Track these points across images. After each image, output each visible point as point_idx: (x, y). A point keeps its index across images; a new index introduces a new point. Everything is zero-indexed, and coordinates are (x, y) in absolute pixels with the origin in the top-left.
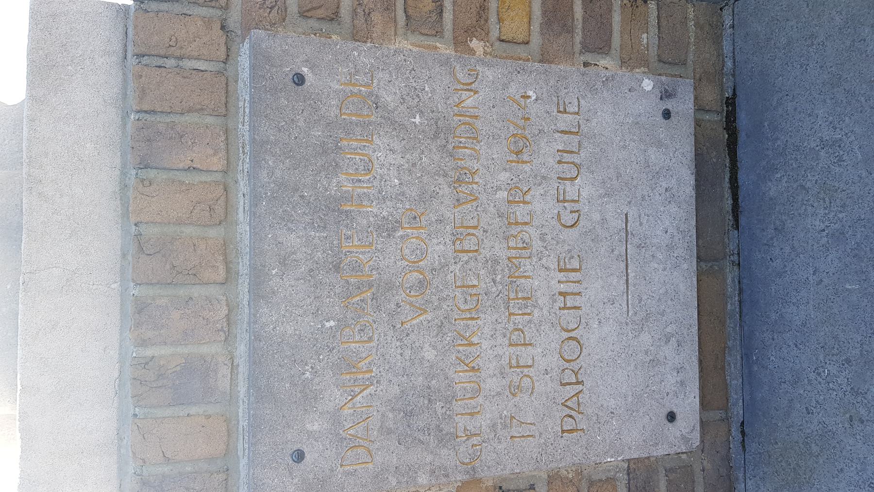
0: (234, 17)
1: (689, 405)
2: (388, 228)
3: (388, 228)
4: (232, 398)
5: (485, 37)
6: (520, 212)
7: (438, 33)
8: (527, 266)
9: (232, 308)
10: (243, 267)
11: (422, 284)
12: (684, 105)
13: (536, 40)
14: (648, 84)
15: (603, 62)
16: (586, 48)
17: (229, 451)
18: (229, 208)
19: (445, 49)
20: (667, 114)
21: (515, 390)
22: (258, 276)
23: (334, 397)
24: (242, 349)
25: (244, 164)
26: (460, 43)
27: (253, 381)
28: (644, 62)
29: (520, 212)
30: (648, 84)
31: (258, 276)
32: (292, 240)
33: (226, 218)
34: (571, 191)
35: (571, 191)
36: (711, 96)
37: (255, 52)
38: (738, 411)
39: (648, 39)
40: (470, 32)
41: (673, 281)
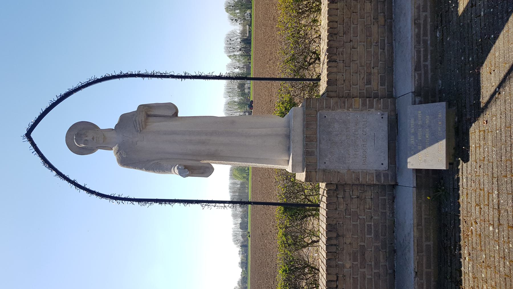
0: (317, 109)
1: (386, 163)
2: (337, 135)
3: (337, 135)
4: (317, 156)
5: (352, 108)
6: (357, 133)
7: (345, 108)
8: (357, 140)
9: (317, 145)
10: (318, 140)
11: (341, 143)
12: (386, 116)
13: (360, 108)
14: (379, 113)
15: (373, 110)
16: (369, 108)
17: (316, 162)
18: (316, 133)
19: (346, 111)
20: (382, 118)
21: (355, 158)
22: (320, 141)
23: (330, 156)
24: (318, 150)
25: (318, 127)
26: (348, 110)
27: (319, 154)
28: (380, 109)
29: (357, 133)
30: (379, 113)
31: (320, 141)
32: (324, 136)
33: (316, 134)
34: (365, 130)
35: (365, 130)
36: (393, 113)
37: (320, 114)
38: (397, 165)
39: (381, 106)
40: (349, 108)
41: (384, 144)
